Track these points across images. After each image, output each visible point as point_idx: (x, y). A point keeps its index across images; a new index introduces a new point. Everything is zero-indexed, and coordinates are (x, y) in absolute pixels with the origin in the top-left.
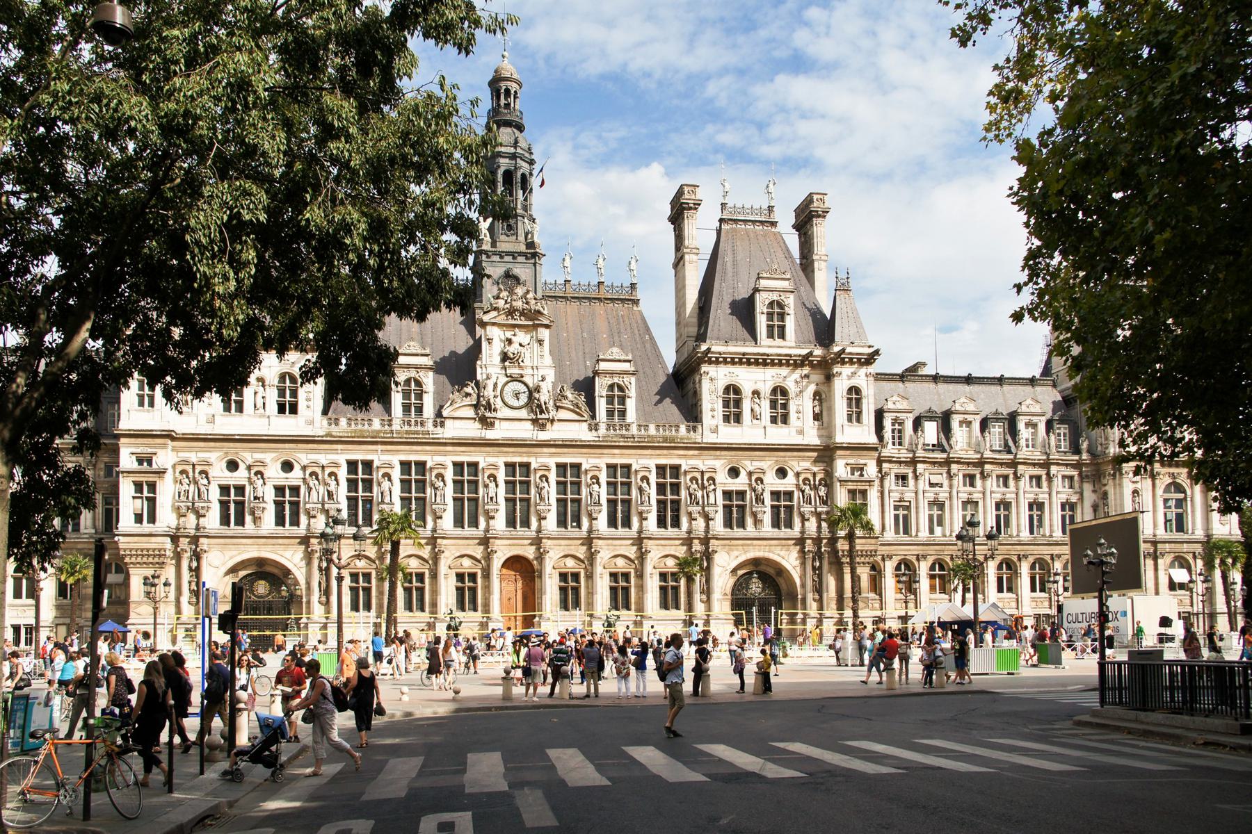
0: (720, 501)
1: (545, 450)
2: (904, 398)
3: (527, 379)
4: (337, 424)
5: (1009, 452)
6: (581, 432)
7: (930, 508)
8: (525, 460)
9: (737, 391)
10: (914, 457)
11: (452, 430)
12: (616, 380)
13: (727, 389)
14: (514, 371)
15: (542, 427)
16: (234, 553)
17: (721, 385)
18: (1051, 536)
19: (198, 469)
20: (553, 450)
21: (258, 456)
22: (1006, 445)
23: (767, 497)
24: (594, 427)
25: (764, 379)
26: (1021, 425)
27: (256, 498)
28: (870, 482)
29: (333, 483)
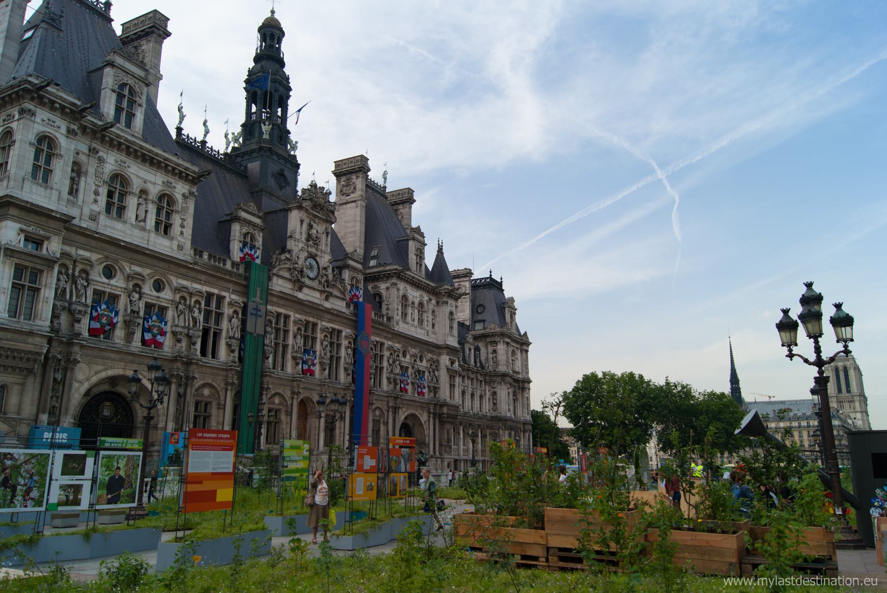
3: (318, 259)
4: (201, 256)
8: (315, 321)
11: (280, 285)
14: (313, 250)
16: (100, 368)
17: (401, 293)
19: (79, 267)
20: (329, 316)
21: (138, 269)
24: (348, 306)
27: (133, 312)
29: (196, 310)
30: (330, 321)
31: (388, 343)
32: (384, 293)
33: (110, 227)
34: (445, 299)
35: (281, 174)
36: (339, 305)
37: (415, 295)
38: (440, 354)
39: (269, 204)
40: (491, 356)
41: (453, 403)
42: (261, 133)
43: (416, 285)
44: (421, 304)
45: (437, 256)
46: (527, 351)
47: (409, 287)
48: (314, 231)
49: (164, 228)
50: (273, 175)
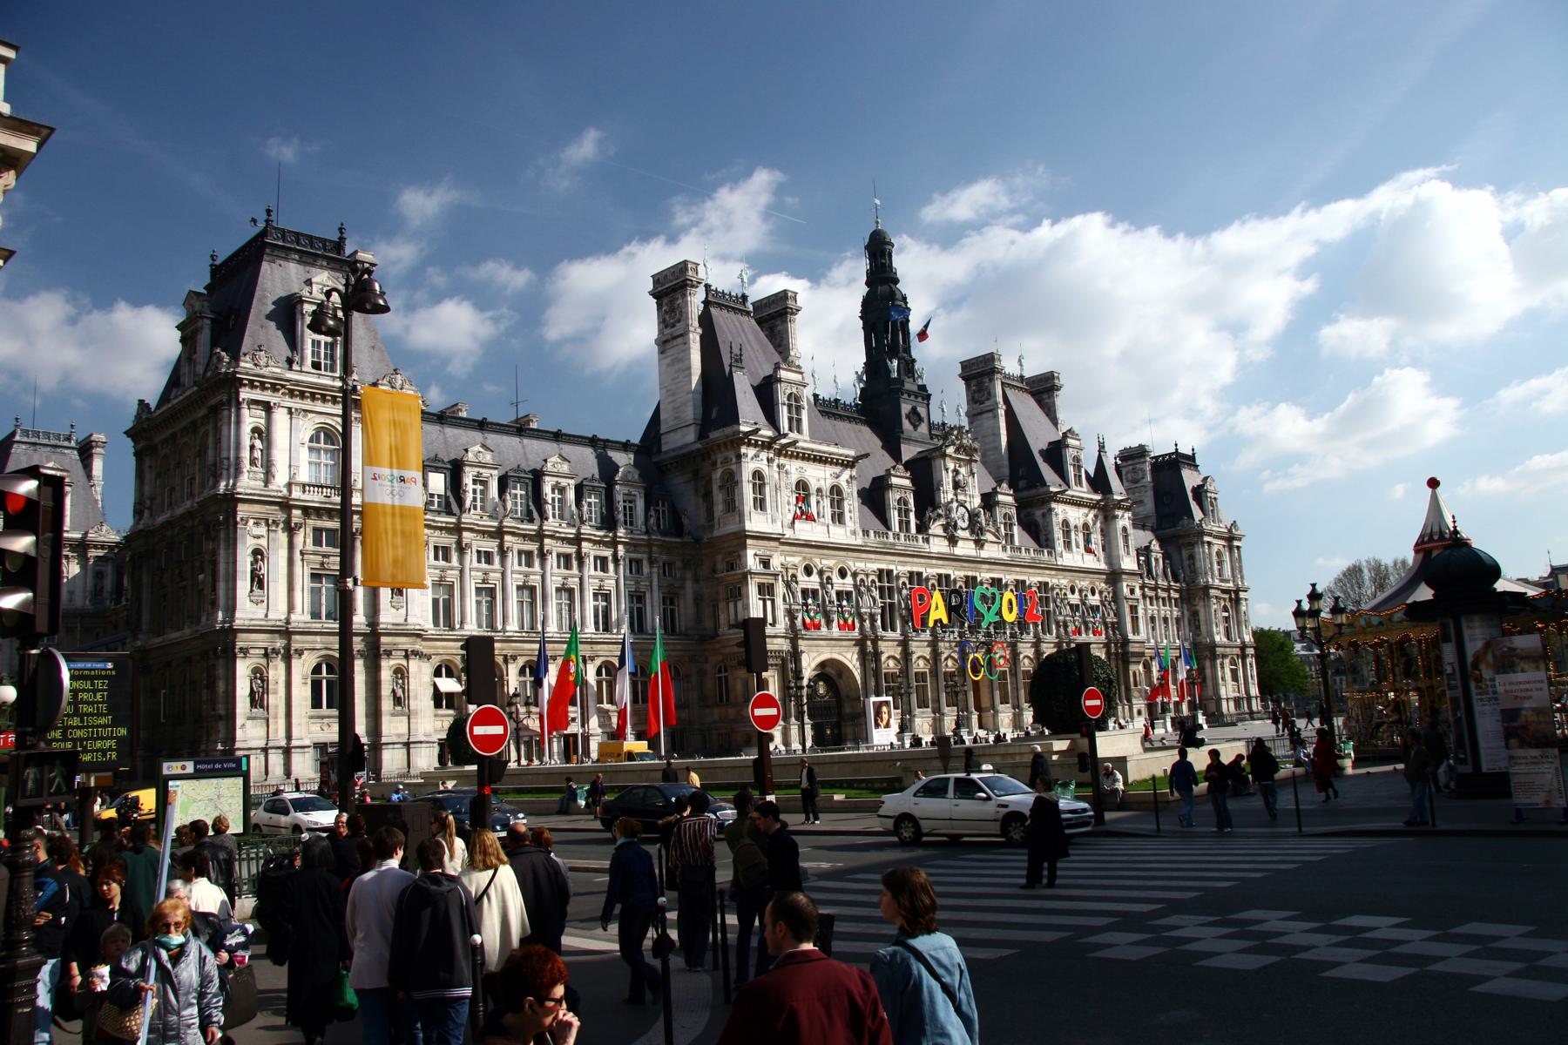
2: (565, 459)
5: (450, 513)
7: (596, 599)
10: (579, 533)
13: (798, 484)
18: (504, 630)
22: (529, 513)
24: (1004, 549)
26: (468, 479)
28: (776, 575)
30: (989, 571)
32: (1040, 520)
33: (805, 531)
35: (914, 410)
36: (992, 551)
39: (908, 452)
40: (1186, 563)
41: (1136, 638)
42: (889, 372)
43: (1078, 503)
44: (1086, 526)
45: (1100, 458)
47: (1068, 508)
48: (960, 477)
49: (838, 518)
50: (908, 417)
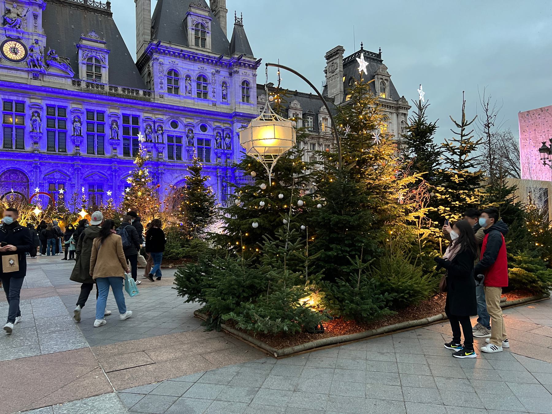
0: (166, 141)
1: (37, 93)
6: (67, 84)
8: (21, 99)
9: (176, 73)
12: (94, 54)
15: (36, 77)
17: (166, 68)
23: (195, 141)
25: (194, 69)
31: (144, 115)
34: (235, 69)
37: (184, 67)
38: (232, 123)
44: (202, 78)
46: (405, 115)
48: (13, 15)
